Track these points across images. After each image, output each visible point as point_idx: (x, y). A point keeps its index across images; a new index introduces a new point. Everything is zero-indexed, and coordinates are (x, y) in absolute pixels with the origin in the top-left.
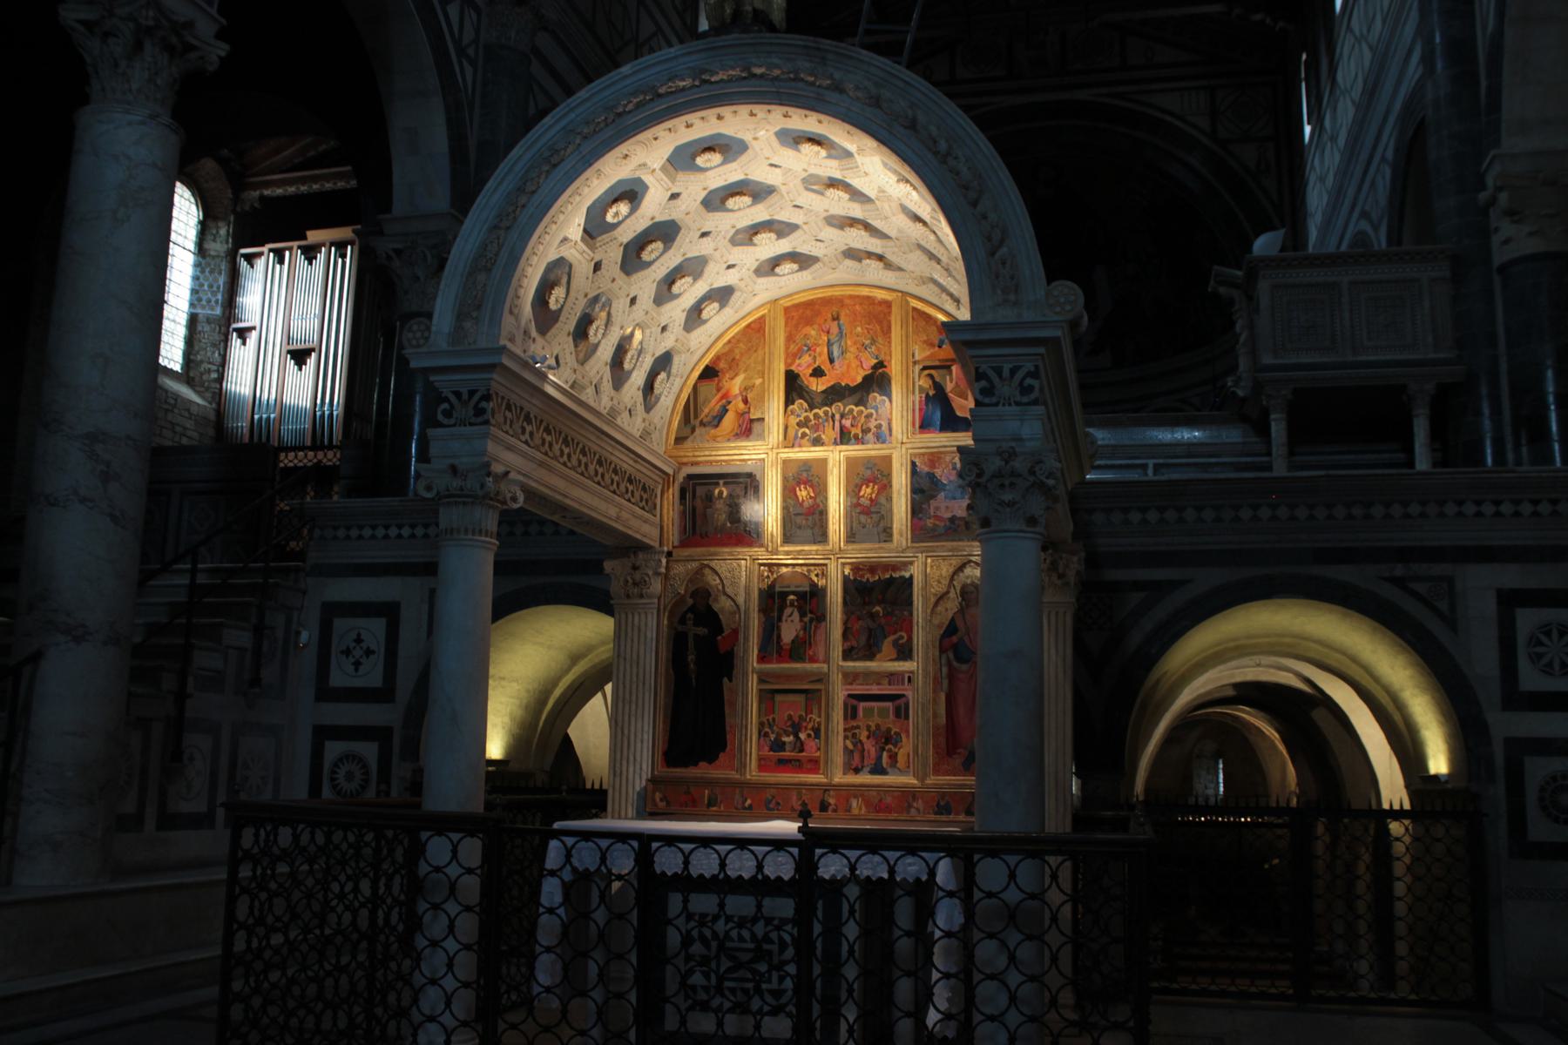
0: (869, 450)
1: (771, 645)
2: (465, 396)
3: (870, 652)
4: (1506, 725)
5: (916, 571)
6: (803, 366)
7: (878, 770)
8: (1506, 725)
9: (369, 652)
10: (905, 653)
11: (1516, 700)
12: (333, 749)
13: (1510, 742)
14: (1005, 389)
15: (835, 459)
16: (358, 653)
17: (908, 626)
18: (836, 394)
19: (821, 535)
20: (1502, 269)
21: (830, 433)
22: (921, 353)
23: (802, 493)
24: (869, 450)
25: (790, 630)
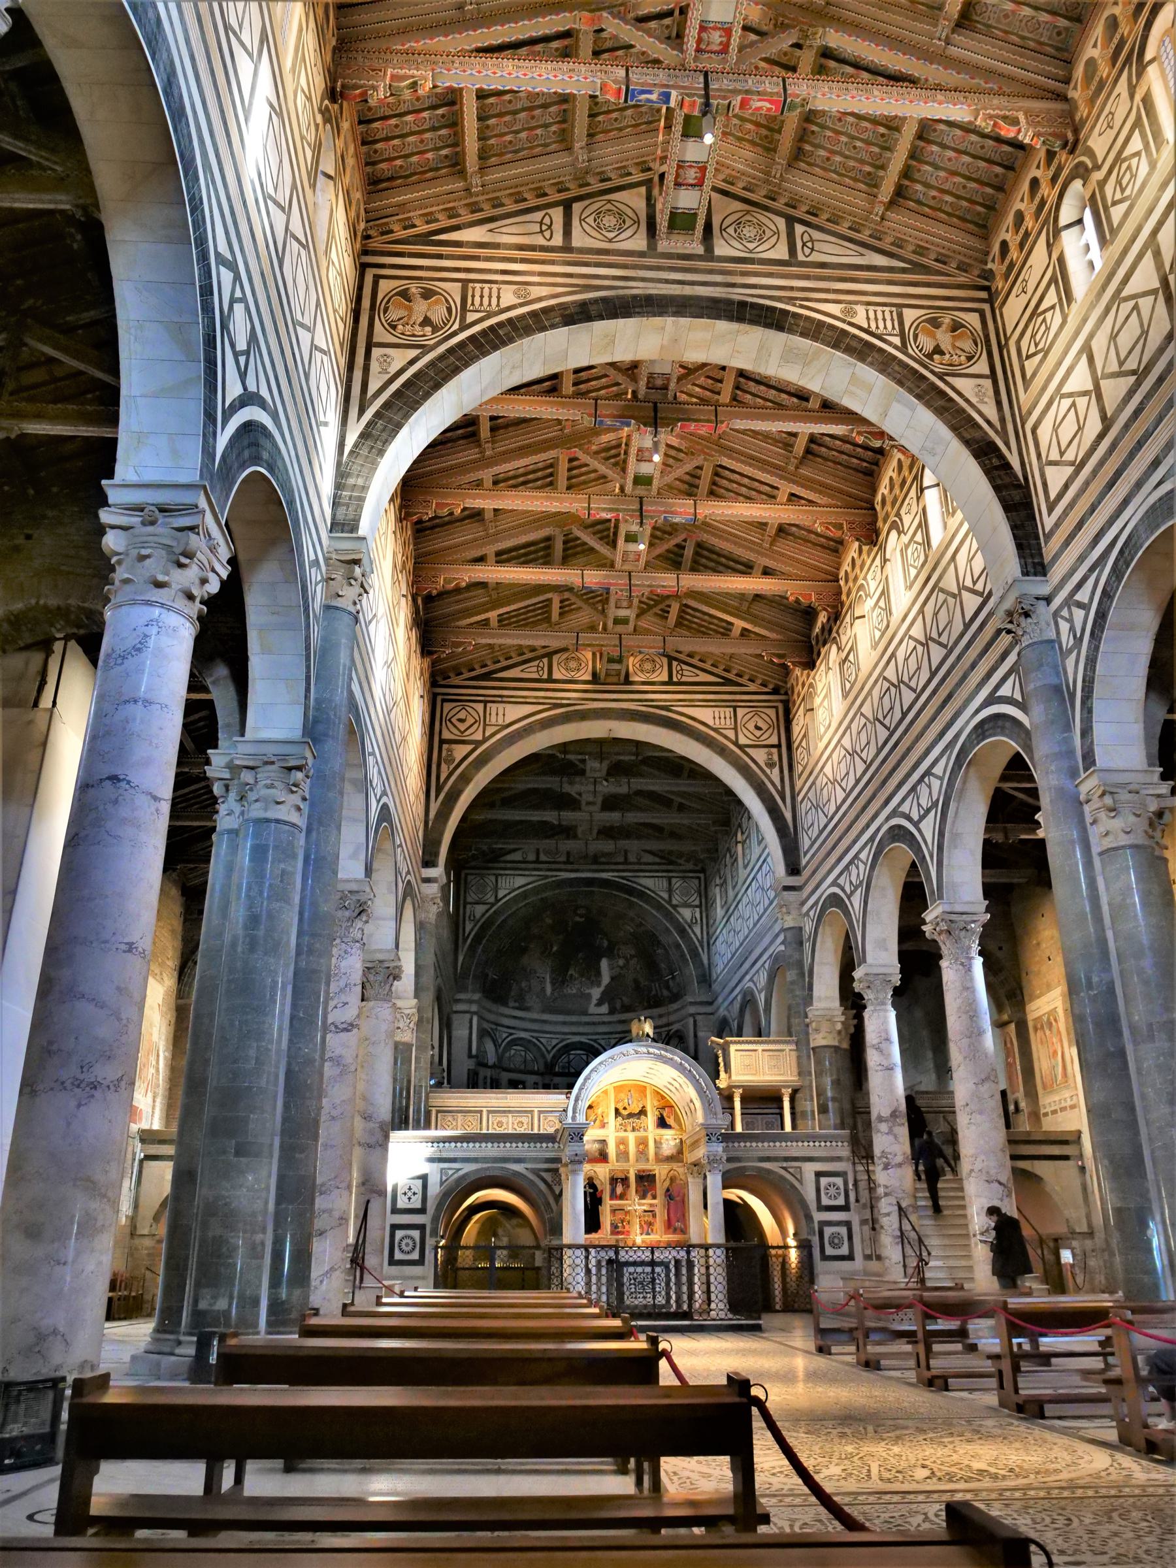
0: (642, 1134)
1: (613, 1196)
3: (643, 1197)
4: (819, 1216)
5: (657, 1172)
6: (620, 1107)
7: (648, 1234)
8: (819, 1216)
9: (414, 1194)
10: (654, 1197)
11: (821, 1208)
12: (399, 1234)
13: (820, 1222)
14: (713, 1139)
15: (631, 1137)
16: (410, 1194)
17: (654, 1188)
18: (631, 1115)
19: (627, 1160)
20: (813, 1049)
21: (629, 1128)
22: (656, 1103)
23: (622, 1147)
24: (642, 1134)
25: (619, 1190)
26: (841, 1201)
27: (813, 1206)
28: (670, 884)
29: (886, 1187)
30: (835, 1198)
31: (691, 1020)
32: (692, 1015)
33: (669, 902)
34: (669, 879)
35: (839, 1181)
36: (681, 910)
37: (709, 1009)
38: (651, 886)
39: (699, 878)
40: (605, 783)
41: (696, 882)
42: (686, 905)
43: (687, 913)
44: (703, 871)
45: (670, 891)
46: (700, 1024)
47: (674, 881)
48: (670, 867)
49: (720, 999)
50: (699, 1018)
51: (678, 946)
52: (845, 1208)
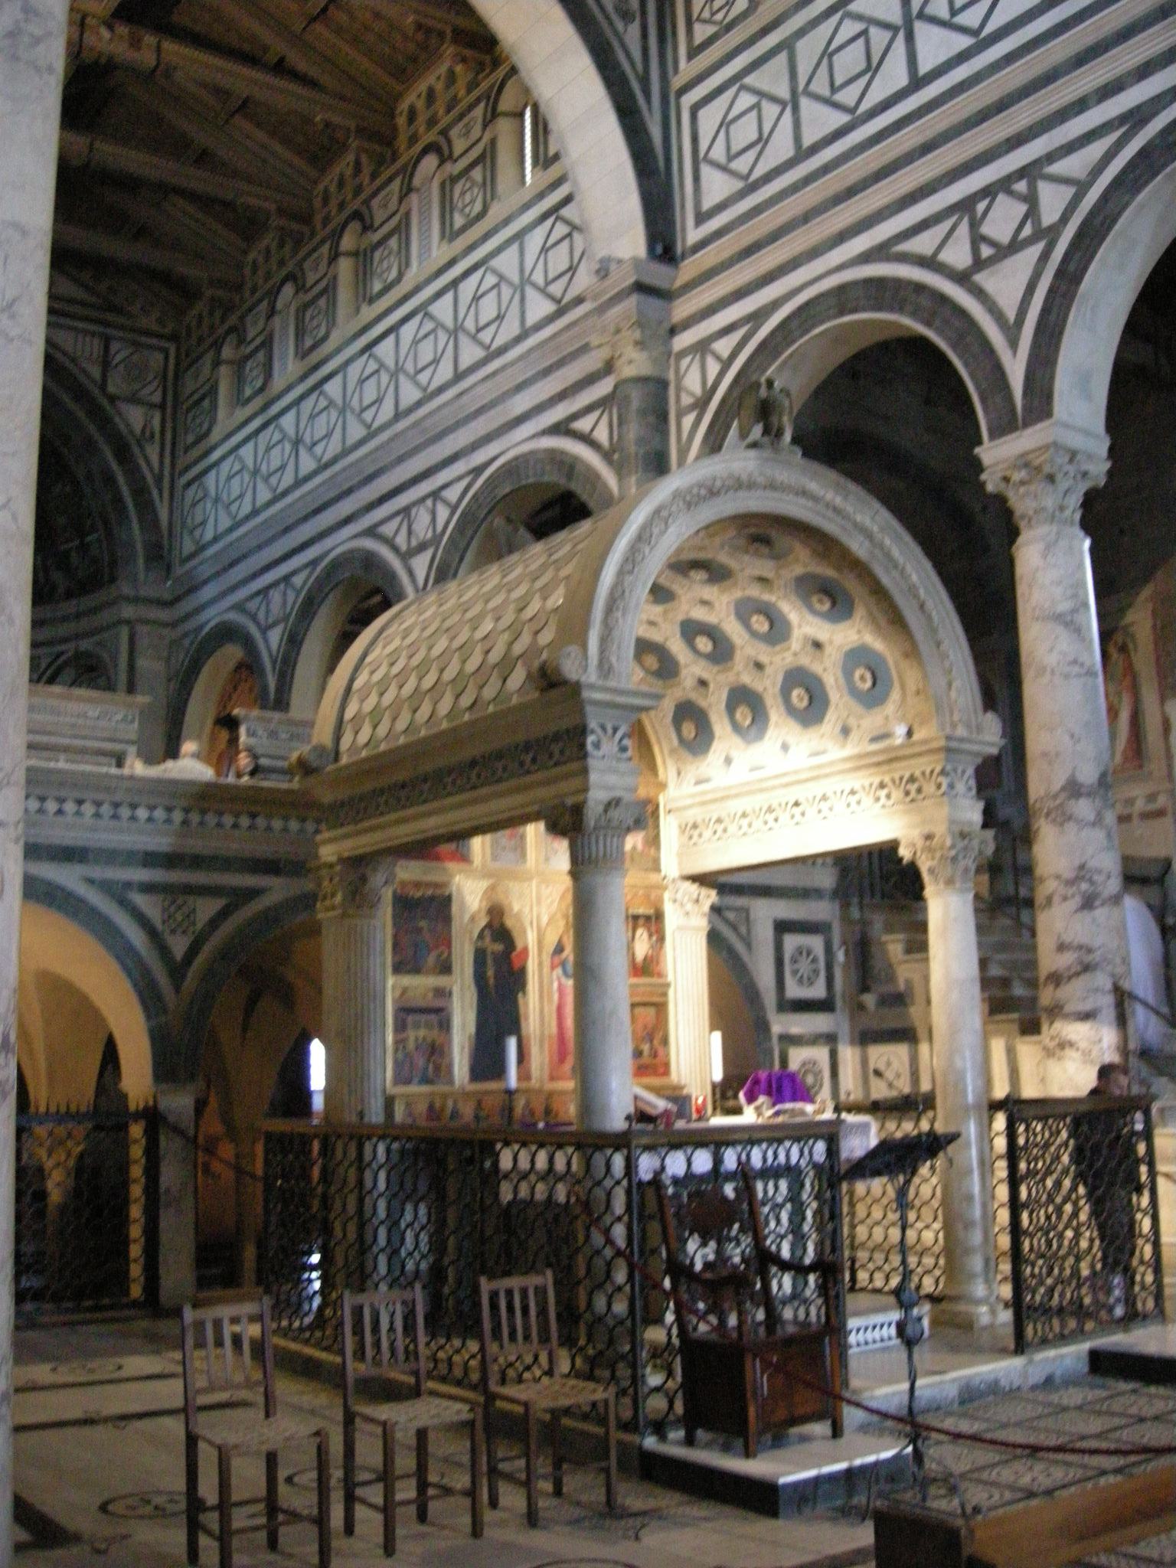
2: (610, 731)
8: (781, 1024)
26: (818, 991)
27: (770, 999)
28: (107, 348)
29: (1090, 951)
30: (811, 983)
31: (124, 633)
32: (128, 622)
33: (103, 387)
34: (107, 341)
35: (816, 943)
36: (126, 408)
37: (164, 615)
38: (70, 349)
39: (166, 353)
40: (105, 33)
41: (160, 357)
42: (134, 399)
43: (135, 417)
44: (174, 337)
45: (106, 364)
46: (143, 643)
47: (114, 346)
48: (110, 317)
49: (207, 592)
50: (142, 629)
51: (110, 480)
52: (824, 1006)
